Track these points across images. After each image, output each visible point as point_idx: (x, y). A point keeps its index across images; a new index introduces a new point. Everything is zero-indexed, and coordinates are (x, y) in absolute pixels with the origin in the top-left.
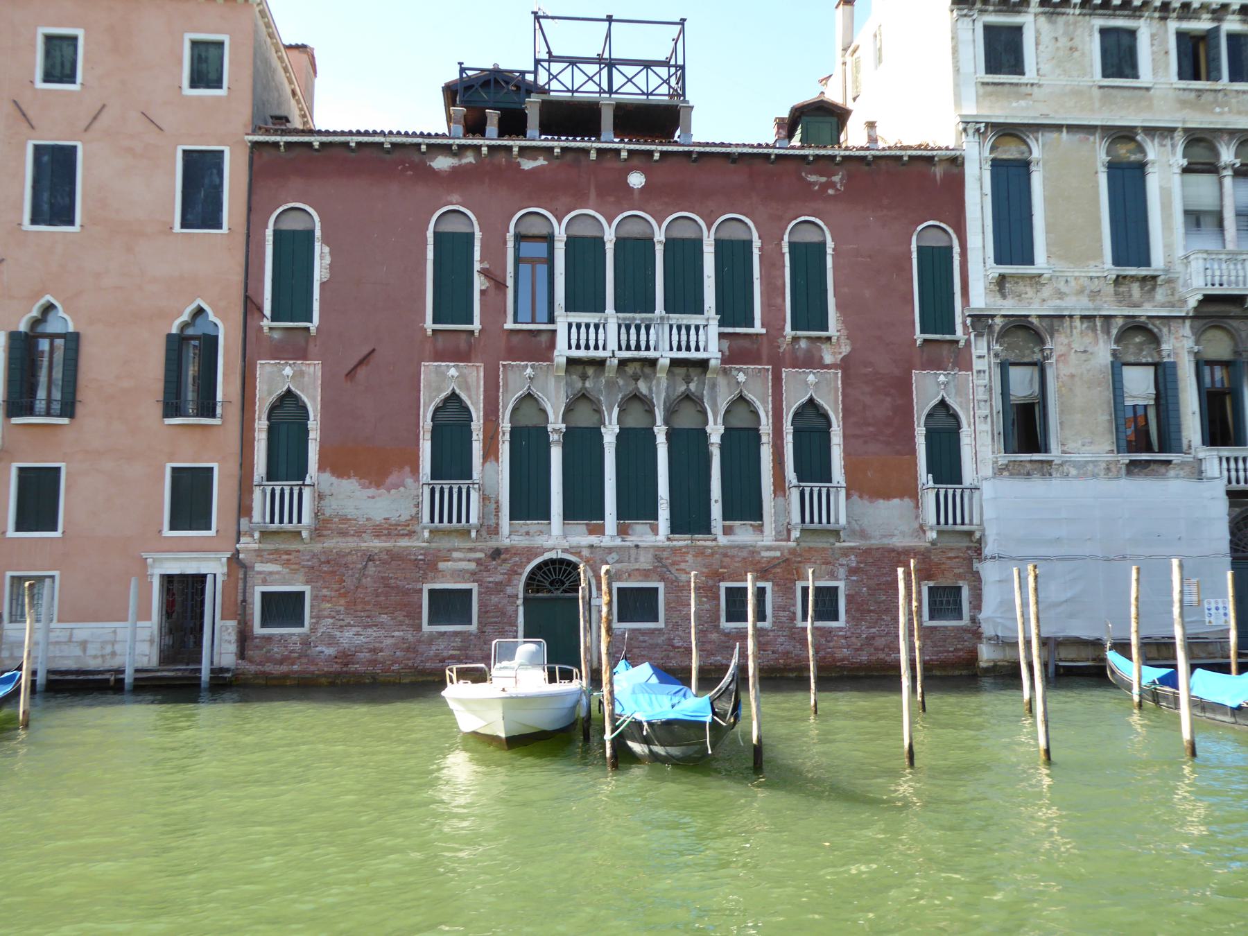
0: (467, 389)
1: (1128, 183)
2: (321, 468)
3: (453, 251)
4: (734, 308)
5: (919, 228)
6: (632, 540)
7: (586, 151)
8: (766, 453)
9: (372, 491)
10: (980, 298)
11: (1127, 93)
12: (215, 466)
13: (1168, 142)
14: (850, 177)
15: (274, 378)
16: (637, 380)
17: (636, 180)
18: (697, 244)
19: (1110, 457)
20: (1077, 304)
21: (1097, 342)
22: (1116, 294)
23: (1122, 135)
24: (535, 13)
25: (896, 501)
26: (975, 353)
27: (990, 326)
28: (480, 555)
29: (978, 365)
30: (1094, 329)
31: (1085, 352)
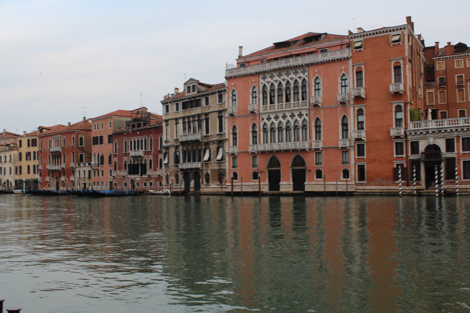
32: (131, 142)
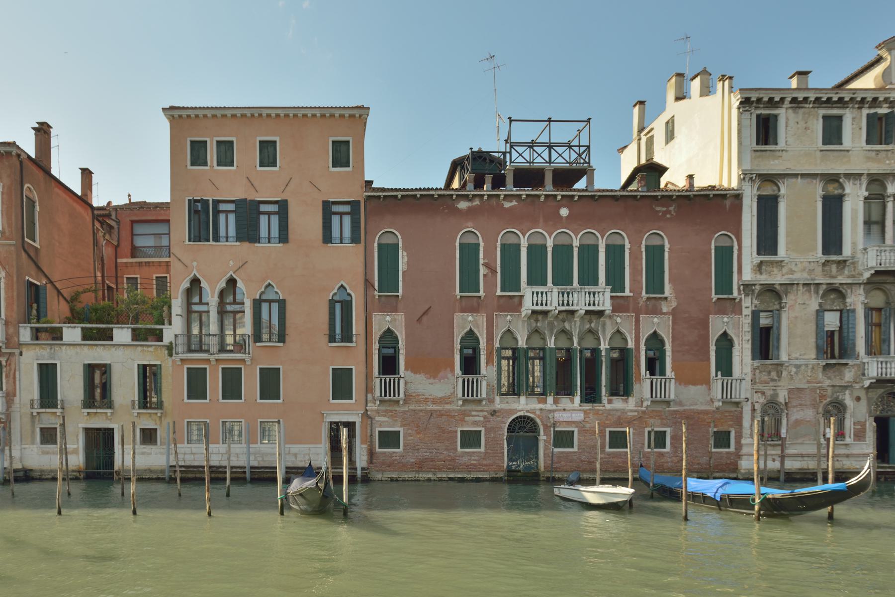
1: (833, 208)
2: (406, 369)
3: (469, 252)
4: (615, 280)
6: (561, 406)
7: (538, 196)
9: (431, 380)
11: (836, 154)
12: (353, 367)
13: (858, 182)
15: (381, 322)
16: (564, 321)
17: (564, 212)
18: (596, 248)
19: (815, 362)
20: (800, 276)
21: (811, 297)
23: (833, 179)
24: (510, 118)
25: (699, 387)
26: (744, 305)
27: (753, 291)
28: (486, 413)
30: (810, 291)
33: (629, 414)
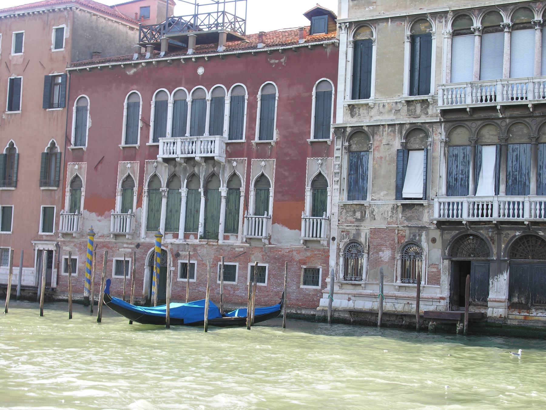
0: (134, 172)
2: (84, 209)
5: (317, 82)
8: (242, 200)
9: (100, 218)
10: (341, 117)
14: (288, 59)
16: (194, 167)
22: (408, 110)
26: (336, 147)
29: (337, 154)
31: (388, 144)
32: (161, 107)
33: (237, 249)
